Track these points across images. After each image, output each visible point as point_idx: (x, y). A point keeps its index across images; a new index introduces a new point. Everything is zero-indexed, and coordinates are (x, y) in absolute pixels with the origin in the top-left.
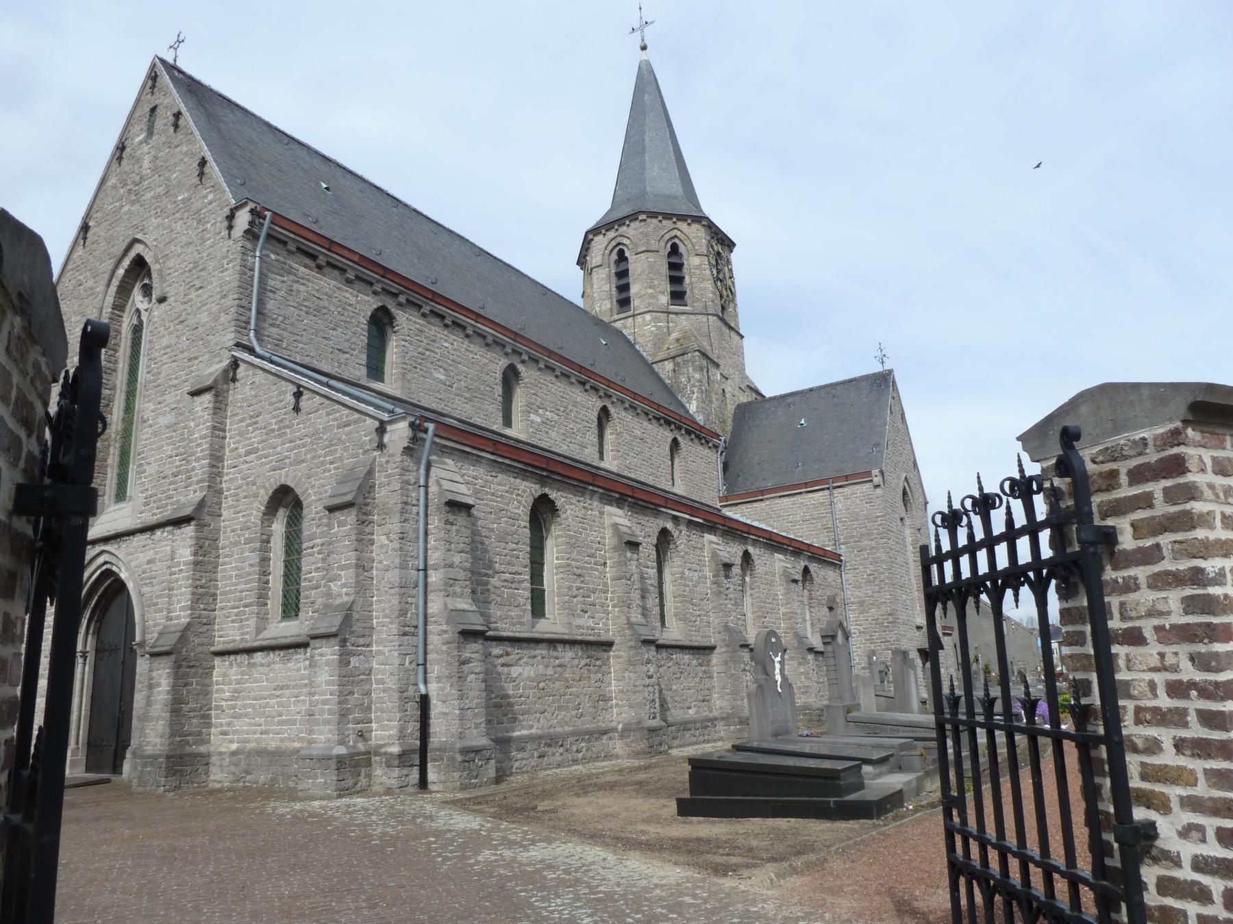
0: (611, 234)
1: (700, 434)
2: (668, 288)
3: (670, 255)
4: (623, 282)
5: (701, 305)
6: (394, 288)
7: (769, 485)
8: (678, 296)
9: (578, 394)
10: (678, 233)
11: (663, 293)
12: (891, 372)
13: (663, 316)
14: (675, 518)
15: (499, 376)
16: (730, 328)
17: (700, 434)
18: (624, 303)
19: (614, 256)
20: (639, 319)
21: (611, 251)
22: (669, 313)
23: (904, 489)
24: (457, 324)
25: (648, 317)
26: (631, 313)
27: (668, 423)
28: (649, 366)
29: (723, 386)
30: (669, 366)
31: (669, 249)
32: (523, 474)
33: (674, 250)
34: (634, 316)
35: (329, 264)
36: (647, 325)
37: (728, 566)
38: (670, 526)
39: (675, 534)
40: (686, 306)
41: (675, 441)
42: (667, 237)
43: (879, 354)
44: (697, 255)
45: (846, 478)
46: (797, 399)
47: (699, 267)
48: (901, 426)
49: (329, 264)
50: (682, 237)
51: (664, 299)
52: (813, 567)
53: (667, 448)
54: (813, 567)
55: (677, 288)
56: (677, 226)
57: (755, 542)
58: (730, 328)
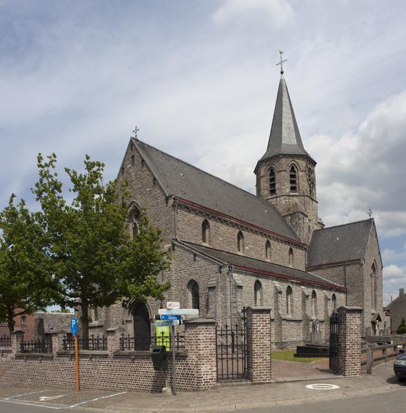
0: (268, 163)
1: (299, 245)
2: (290, 185)
3: (291, 171)
4: (273, 183)
6: (208, 213)
7: (324, 262)
8: (293, 189)
9: (260, 238)
12: (373, 219)
13: (288, 197)
14: (292, 282)
15: (236, 236)
16: (313, 200)
17: (299, 245)
18: (273, 191)
19: (269, 172)
20: (278, 199)
22: (289, 196)
23: (373, 264)
24: (226, 221)
25: (282, 198)
26: (275, 196)
27: (289, 243)
30: (289, 218)
32: (253, 275)
33: (293, 170)
34: (276, 197)
35: (192, 210)
37: (308, 296)
38: (290, 285)
39: (292, 287)
41: (291, 249)
43: (369, 212)
45: (351, 261)
46: (337, 229)
48: (375, 239)
49: (192, 210)
51: (288, 190)
52: (336, 294)
53: (288, 251)
54: (336, 294)
55: (293, 185)
57: (317, 287)
58: (313, 200)
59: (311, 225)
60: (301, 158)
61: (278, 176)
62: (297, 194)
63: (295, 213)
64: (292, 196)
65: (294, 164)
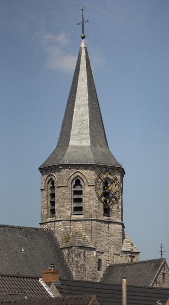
5: (89, 214)
8: (78, 209)
10: (79, 174)
11: (69, 209)
13: (68, 223)
18: (53, 212)
20: (57, 223)
21: (48, 182)
25: (60, 223)
28: (58, 251)
29: (99, 257)
31: (74, 183)
34: (55, 221)
36: (60, 227)
40: (82, 215)
42: (73, 177)
44: (89, 186)
47: (89, 193)
50: (81, 176)
56: (79, 170)
59: (103, 258)
60: (90, 168)
61: (58, 193)
62: (81, 217)
63: (72, 247)
64: (75, 221)
65: (78, 176)
